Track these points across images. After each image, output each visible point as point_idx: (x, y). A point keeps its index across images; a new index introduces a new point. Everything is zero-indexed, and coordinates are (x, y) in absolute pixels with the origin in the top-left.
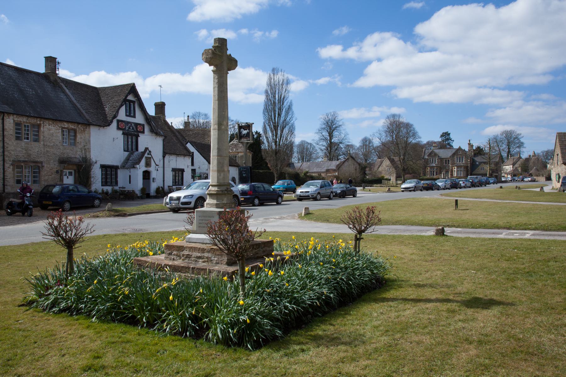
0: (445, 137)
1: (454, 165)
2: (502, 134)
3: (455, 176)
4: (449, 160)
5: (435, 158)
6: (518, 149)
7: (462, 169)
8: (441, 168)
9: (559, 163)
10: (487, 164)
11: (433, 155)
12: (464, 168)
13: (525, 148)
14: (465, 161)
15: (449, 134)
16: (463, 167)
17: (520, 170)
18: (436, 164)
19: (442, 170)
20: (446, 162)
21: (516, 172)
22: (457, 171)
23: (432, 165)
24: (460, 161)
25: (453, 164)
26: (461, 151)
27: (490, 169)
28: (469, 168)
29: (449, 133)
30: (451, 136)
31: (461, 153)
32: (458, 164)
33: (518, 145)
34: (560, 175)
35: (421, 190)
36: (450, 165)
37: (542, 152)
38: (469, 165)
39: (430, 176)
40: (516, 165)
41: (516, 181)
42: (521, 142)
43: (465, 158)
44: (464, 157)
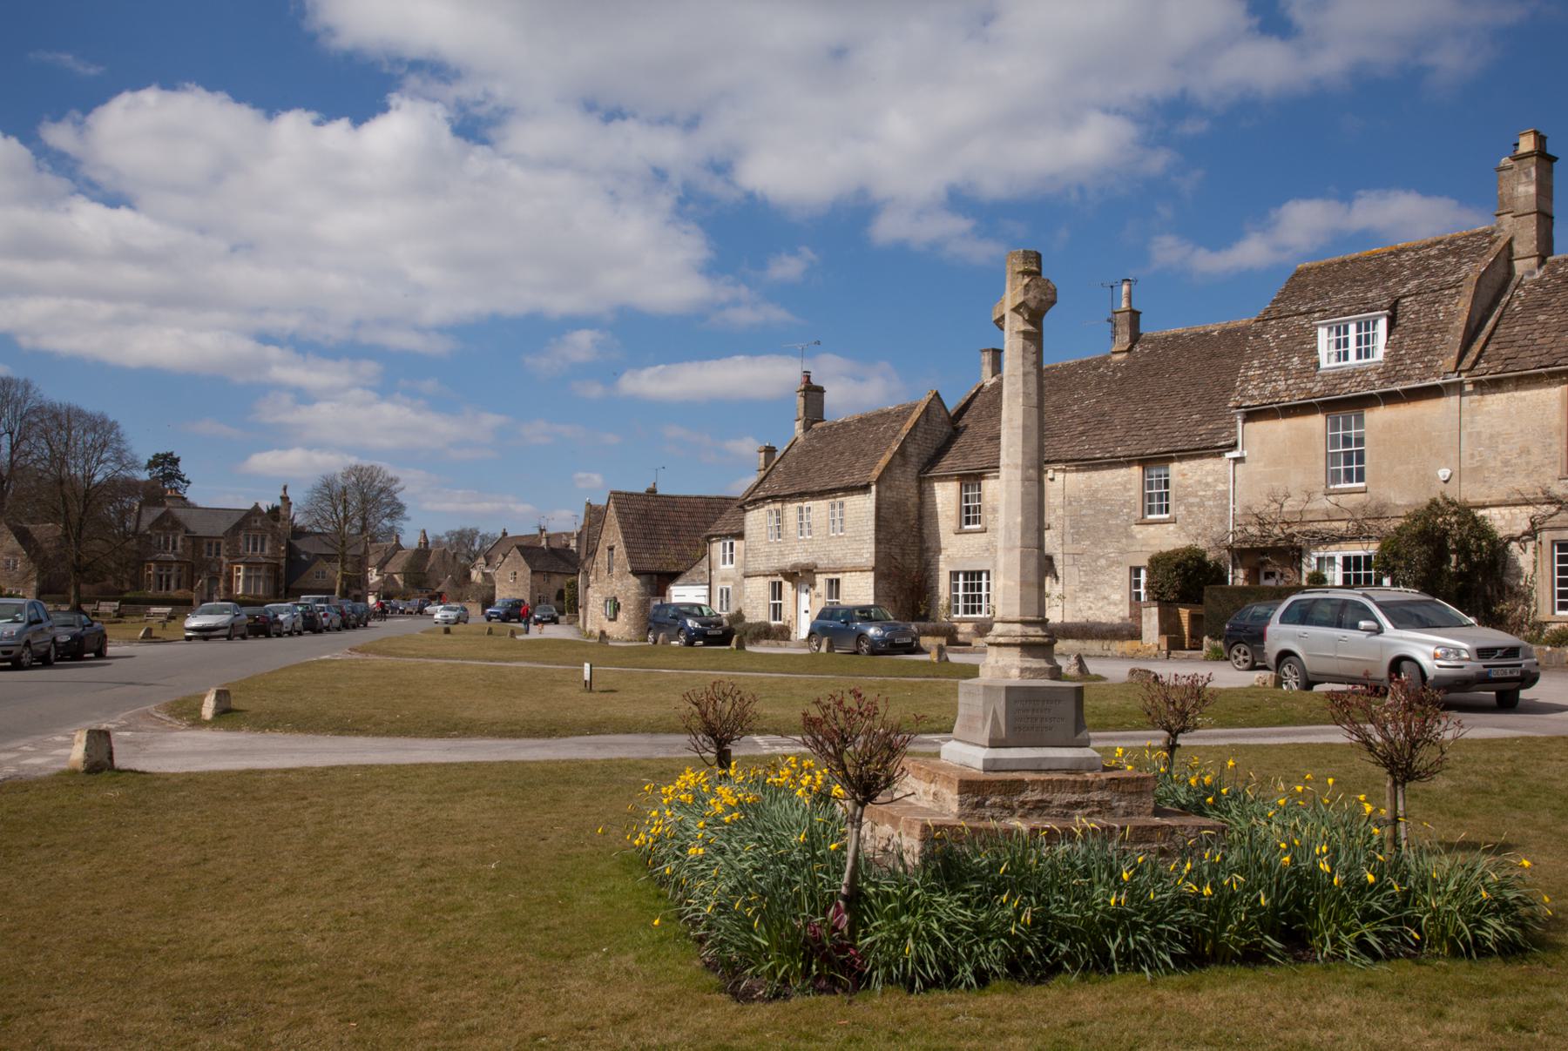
0: (163, 470)
1: (237, 560)
2: (346, 477)
3: (240, 592)
4: (218, 544)
5: (176, 535)
6: (386, 522)
7: (262, 573)
8: (193, 565)
9: (615, 570)
10: (336, 561)
11: (169, 524)
12: (268, 571)
13: (408, 519)
14: (271, 549)
15: (176, 461)
16: (264, 567)
17: (401, 583)
18: (176, 555)
19: (196, 574)
20: (210, 549)
21: (391, 588)
22: (247, 578)
23: (162, 556)
24: (255, 549)
25: (234, 556)
26: (259, 519)
27: (344, 577)
28: (282, 571)
29: (175, 456)
30: (183, 468)
31: (258, 524)
32: (248, 557)
33: (388, 511)
34: (619, 600)
35: (244, 637)
36: (226, 561)
37: (447, 534)
38: (283, 562)
39: (155, 591)
40: (390, 568)
41: (402, 612)
42: (398, 504)
43: (272, 541)
44: (269, 537)
